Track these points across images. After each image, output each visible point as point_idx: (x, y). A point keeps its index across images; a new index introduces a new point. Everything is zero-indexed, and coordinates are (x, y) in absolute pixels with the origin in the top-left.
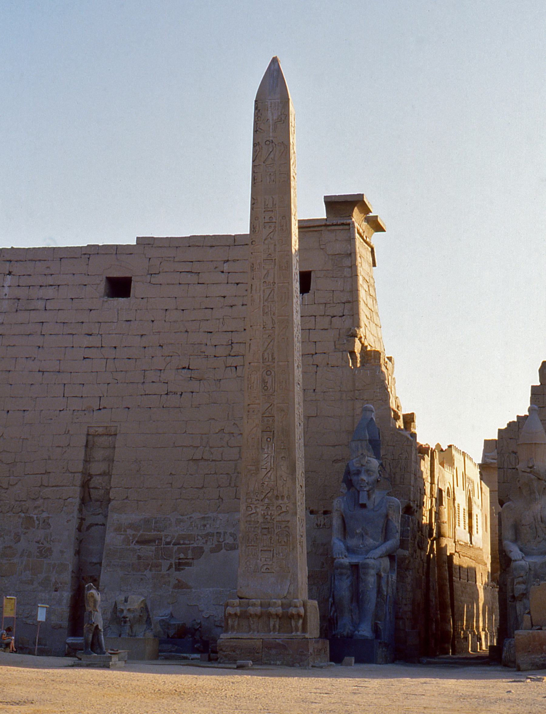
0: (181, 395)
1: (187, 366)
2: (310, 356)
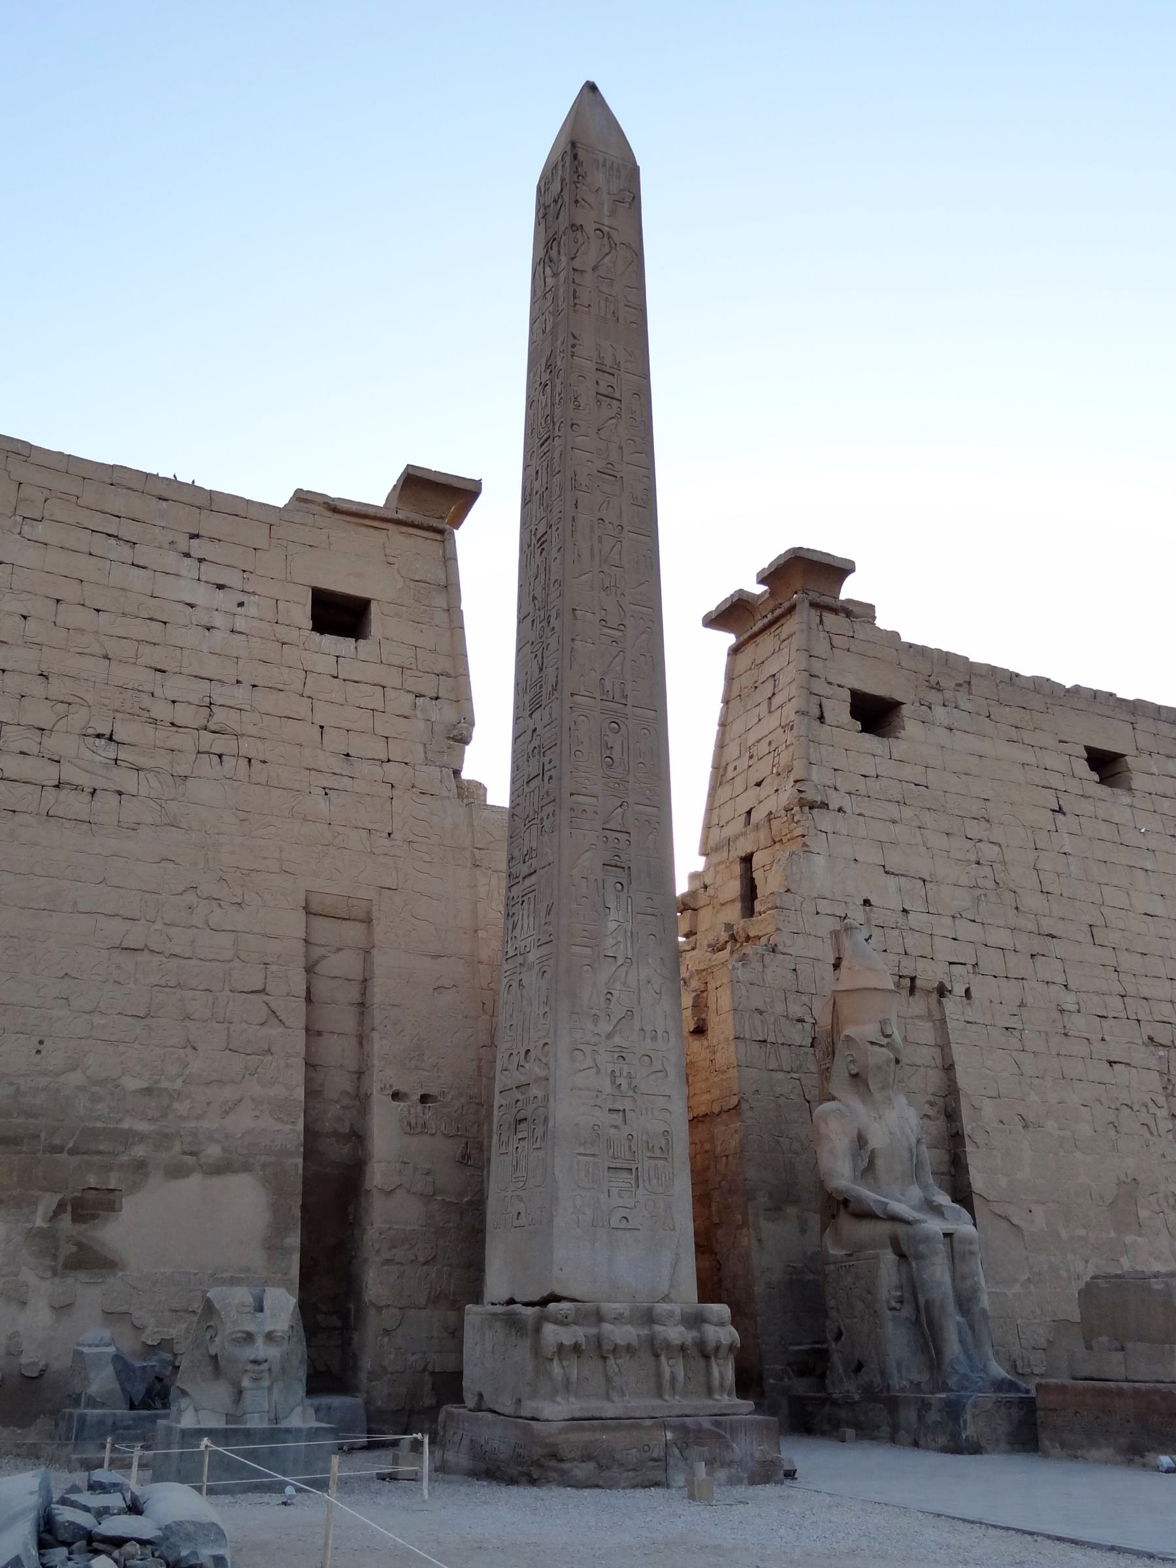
0: (93, 793)
1: (107, 732)
2: (378, 763)
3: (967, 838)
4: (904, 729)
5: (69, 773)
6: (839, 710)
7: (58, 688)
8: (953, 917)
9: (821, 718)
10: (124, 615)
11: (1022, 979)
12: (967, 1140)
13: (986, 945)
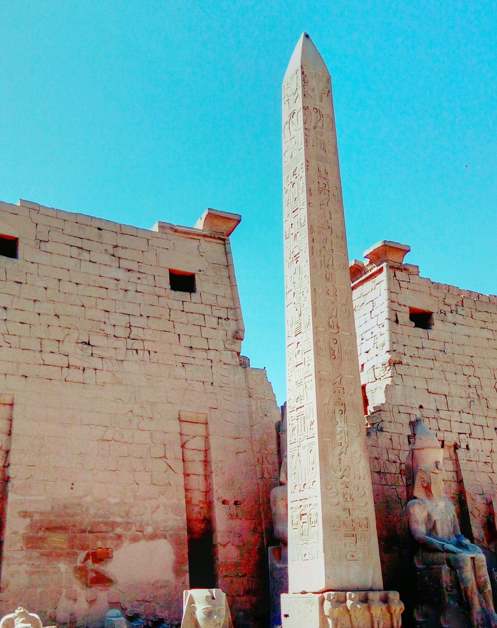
0: (84, 370)
1: (87, 341)
3: (464, 375)
4: (434, 325)
5: (73, 361)
6: (405, 317)
7: (64, 321)
8: (460, 412)
9: (397, 321)
10: (89, 285)
11: (491, 440)
12: (470, 515)
13: (475, 424)
